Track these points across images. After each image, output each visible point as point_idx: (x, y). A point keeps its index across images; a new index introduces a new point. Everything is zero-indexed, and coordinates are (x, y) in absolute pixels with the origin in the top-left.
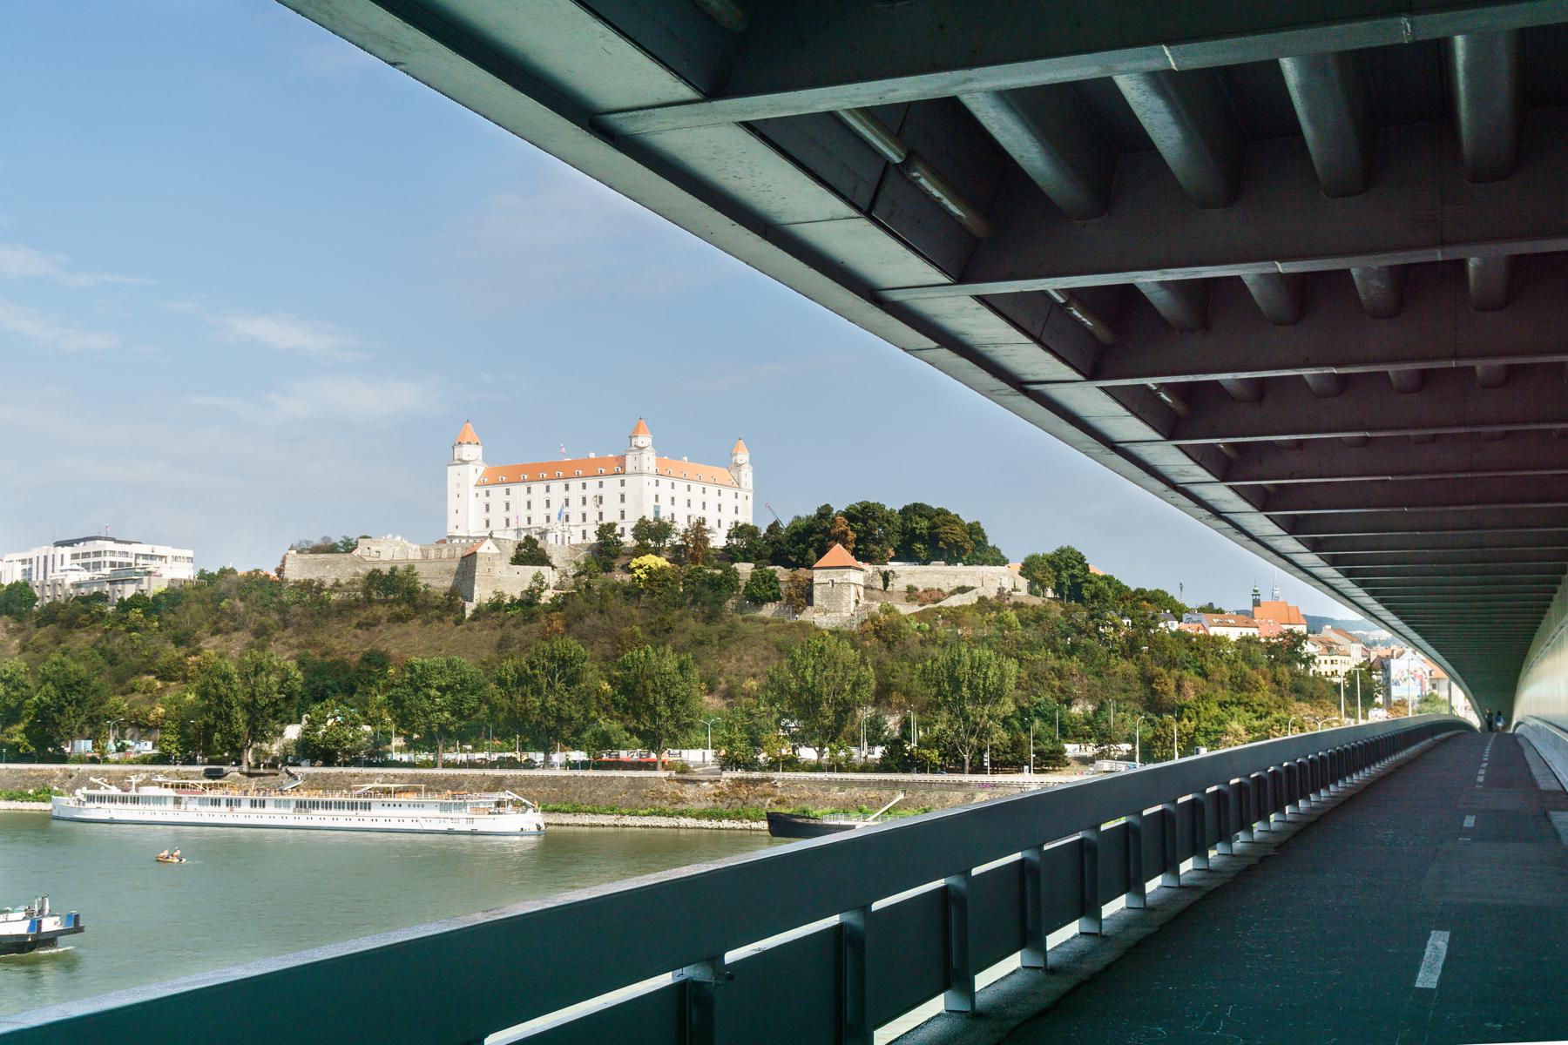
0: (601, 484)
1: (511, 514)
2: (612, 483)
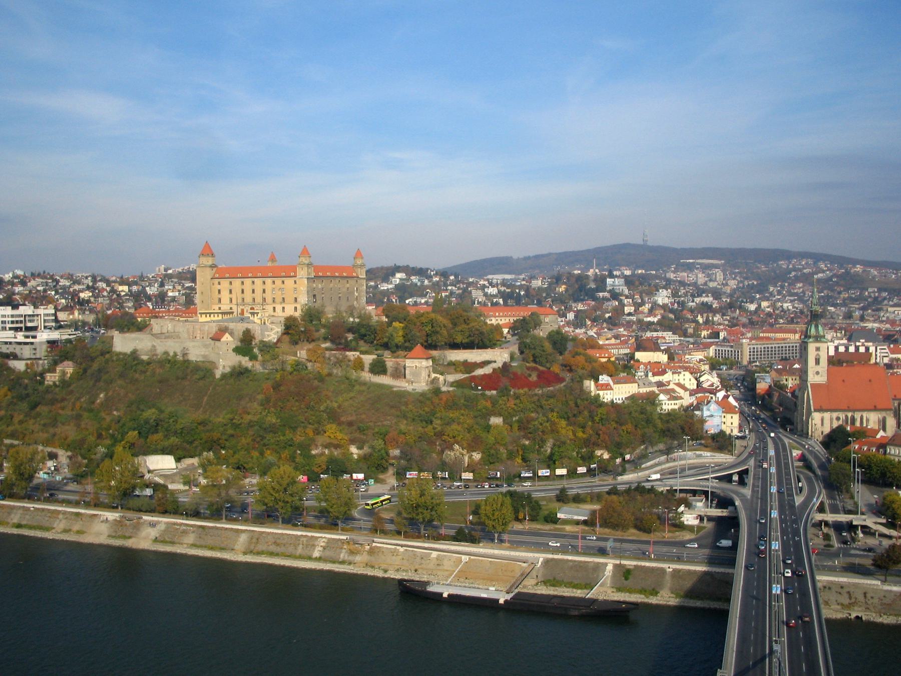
0: (283, 282)
1: (234, 296)
2: (289, 282)
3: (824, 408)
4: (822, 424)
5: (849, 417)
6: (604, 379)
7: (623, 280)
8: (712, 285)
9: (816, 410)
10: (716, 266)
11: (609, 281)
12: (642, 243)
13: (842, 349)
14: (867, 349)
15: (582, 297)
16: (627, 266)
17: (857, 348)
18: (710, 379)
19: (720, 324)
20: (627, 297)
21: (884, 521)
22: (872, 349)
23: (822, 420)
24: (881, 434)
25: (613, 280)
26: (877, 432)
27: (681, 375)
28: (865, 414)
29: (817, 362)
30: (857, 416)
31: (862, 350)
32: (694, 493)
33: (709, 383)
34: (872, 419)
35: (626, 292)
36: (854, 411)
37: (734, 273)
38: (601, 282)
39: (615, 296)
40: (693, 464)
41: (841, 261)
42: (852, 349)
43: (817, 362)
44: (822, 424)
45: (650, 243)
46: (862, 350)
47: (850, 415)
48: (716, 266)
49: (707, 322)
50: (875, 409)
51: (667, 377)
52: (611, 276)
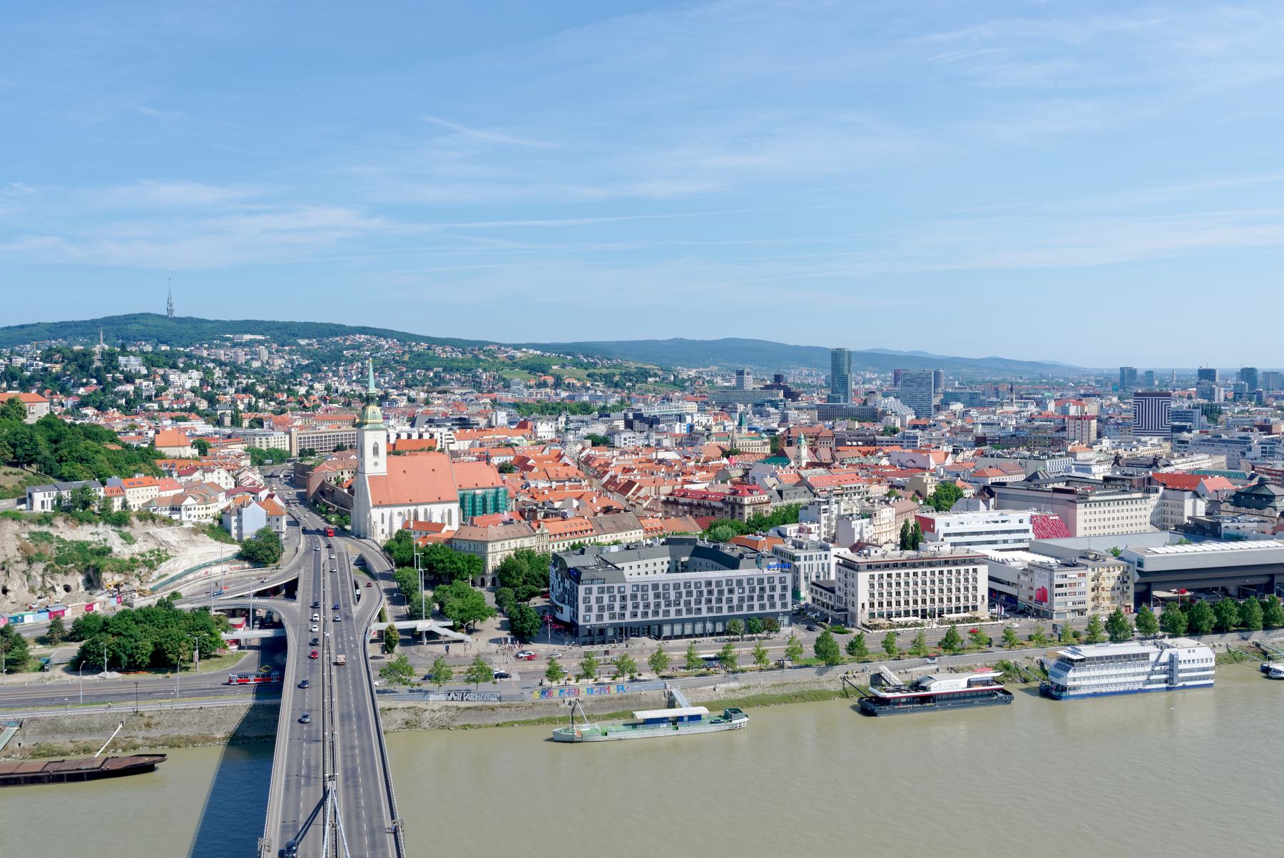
3: (383, 503)
4: (383, 522)
5: (412, 512)
6: (115, 480)
7: (140, 359)
8: (256, 364)
9: (374, 506)
10: (261, 343)
11: (122, 360)
12: (164, 313)
13: (404, 436)
14: (432, 436)
15: (85, 380)
16: (146, 340)
17: (421, 436)
18: (253, 476)
19: (265, 410)
20: (146, 377)
21: (451, 624)
22: (437, 436)
23: (383, 514)
24: (447, 528)
25: (126, 358)
26: (443, 525)
27: (216, 473)
28: (428, 507)
29: (376, 451)
30: (421, 509)
31: (426, 436)
32: (233, 613)
33: (250, 481)
34: (437, 513)
35: (144, 371)
36: (417, 504)
37: (282, 351)
38: (110, 358)
39: (129, 379)
40: (13, 684)
41: (404, 338)
42: (415, 436)
43: (376, 451)
44: (383, 522)
45: (176, 314)
46: (426, 436)
47: (412, 509)
48: (261, 343)
49: (250, 408)
50: (440, 501)
51: (197, 476)
52: (124, 352)
